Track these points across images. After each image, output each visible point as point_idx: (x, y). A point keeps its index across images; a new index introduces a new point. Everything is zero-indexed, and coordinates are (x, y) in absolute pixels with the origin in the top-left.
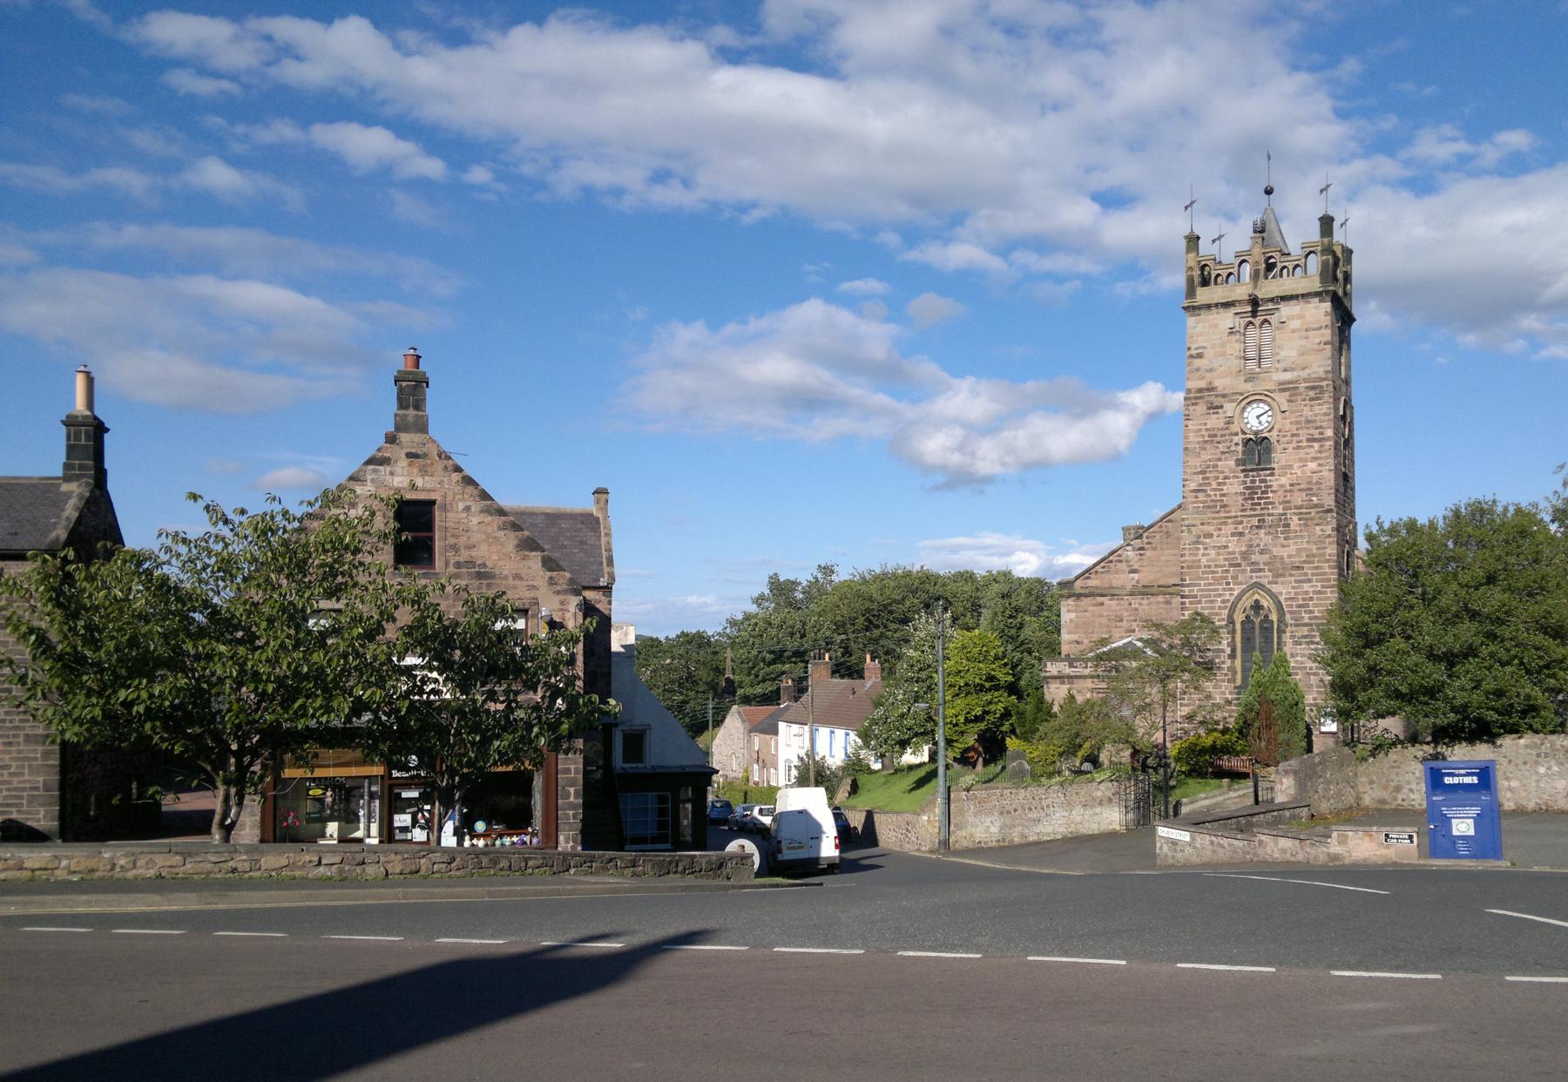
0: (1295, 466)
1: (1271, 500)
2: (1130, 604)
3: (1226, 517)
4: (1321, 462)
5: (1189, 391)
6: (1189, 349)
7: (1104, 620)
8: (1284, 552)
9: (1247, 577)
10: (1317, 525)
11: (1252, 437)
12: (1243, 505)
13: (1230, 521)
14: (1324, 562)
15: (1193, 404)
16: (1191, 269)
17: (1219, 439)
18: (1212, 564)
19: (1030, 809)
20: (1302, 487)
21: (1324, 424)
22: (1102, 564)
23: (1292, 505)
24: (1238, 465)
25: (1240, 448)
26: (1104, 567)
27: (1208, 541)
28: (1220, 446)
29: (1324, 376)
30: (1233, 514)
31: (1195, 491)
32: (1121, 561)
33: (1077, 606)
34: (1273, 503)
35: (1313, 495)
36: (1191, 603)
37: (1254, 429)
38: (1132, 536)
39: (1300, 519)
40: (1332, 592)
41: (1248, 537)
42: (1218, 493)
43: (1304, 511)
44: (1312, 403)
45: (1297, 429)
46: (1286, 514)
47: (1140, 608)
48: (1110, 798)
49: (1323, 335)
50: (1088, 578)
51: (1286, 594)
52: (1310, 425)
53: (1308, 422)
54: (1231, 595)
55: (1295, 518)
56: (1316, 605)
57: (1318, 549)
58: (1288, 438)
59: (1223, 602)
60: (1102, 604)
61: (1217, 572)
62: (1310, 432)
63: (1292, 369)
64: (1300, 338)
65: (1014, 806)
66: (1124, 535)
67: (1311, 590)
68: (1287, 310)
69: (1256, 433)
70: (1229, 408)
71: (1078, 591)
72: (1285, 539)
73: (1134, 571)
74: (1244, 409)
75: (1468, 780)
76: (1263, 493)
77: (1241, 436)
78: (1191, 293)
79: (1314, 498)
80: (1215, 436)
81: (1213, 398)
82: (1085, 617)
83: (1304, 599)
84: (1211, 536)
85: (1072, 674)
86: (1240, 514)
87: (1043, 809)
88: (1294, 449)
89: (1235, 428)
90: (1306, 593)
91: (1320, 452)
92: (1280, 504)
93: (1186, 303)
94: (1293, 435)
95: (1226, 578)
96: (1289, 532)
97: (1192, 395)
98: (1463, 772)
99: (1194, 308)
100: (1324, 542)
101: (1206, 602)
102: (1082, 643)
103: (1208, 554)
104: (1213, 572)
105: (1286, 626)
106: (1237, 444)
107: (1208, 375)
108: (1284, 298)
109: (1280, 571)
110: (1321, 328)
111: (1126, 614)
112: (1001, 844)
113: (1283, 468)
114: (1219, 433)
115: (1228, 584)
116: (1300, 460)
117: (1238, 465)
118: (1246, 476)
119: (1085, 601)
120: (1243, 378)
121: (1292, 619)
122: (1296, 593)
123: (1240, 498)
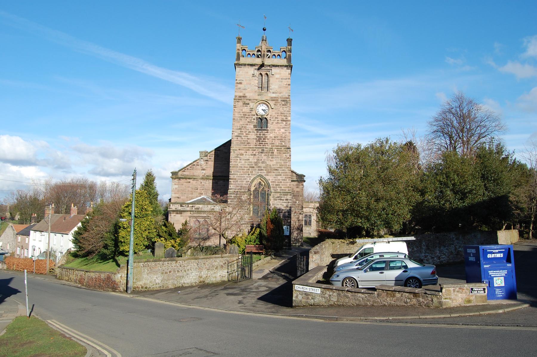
0: (276, 130)
1: (267, 142)
2: (201, 183)
4: (286, 129)
5: (236, 96)
6: (236, 80)
7: (190, 189)
8: (271, 163)
9: (256, 172)
10: (284, 153)
11: (260, 117)
12: (256, 144)
13: (250, 149)
15: (237, 102)
16: (239, 50)
17: (247, 116)
19: (178, 271)
20: (278, 138)
21: (287, 115)
22: (190, 166)
23: (275, 145)
24: (254, 128)
25: (255, 121)
26: (191, 167)
27: (241, 156)
28: (247, 119)
29: (288, 97)
30: (252, 147)
31: (236, 136)
32: (198, 165)
33: (179, 182)
34: (268, 144)
36: (233, 182)
37: (261, 114)
38: (203, 155)
39: (277, 151)
40: (289, 180)
41: (257, 156)
42: (246, 138)
43: (279, 147)
44: (283, 106)
45: (277, 116)
46: (272, 148)
48: (222, 266)
49: (288, 82)
50: (184, 171)
51: (272, 180)
52: (282, 115)
53: (282, 113)
54: (250, 179)
55: (276, 150)
56: (283, 185)
57: (284, 163)
59: (247, 182)
60: (190, 182)
61: (245, 170)
63: (276, 93)
65: (170, 270)
66: (200, 155)
67: (281, 179)
68: (274, 70)
69: (262, 116)
70: (252, 105)
71: (180, 176)
72: (272, 158)
73: (203, 170)
74: (257, 106)
75: (498, 255)
76: (263, 139)
78: (238, 58)
79: (283, 143)
80: (246, 115)
81: (245, 100)
82: (182, 187)
83: (278, 182)
84: (243, 155)
85: (181, 210)
86: (254, 147)
87: (185, 271)
88: (276, 123)
89: (254, 113)
90: (279, 180)
91: (286, 125)
92: (270, 144)
94: (276, 118)
96: (273, 155)
97: (237, 98)
98: (497, 251)
99: (239, 65)
100: (286, 160)
101: (240, 182)
102: (180, 198)
103: (241, 162)
104: (243, 169)
105: (271, 192)
106: (254, 119)
107: (244, 91)
108: (274, 66)
109: (270, 171)
110: (287, 79)
111: (199, 187)
113: (272, 130)
114: (247, 114)
115: (249, 174)
116: (278, 128)
118: (257, 132)
119: (182, 181)
123: (255, 141)
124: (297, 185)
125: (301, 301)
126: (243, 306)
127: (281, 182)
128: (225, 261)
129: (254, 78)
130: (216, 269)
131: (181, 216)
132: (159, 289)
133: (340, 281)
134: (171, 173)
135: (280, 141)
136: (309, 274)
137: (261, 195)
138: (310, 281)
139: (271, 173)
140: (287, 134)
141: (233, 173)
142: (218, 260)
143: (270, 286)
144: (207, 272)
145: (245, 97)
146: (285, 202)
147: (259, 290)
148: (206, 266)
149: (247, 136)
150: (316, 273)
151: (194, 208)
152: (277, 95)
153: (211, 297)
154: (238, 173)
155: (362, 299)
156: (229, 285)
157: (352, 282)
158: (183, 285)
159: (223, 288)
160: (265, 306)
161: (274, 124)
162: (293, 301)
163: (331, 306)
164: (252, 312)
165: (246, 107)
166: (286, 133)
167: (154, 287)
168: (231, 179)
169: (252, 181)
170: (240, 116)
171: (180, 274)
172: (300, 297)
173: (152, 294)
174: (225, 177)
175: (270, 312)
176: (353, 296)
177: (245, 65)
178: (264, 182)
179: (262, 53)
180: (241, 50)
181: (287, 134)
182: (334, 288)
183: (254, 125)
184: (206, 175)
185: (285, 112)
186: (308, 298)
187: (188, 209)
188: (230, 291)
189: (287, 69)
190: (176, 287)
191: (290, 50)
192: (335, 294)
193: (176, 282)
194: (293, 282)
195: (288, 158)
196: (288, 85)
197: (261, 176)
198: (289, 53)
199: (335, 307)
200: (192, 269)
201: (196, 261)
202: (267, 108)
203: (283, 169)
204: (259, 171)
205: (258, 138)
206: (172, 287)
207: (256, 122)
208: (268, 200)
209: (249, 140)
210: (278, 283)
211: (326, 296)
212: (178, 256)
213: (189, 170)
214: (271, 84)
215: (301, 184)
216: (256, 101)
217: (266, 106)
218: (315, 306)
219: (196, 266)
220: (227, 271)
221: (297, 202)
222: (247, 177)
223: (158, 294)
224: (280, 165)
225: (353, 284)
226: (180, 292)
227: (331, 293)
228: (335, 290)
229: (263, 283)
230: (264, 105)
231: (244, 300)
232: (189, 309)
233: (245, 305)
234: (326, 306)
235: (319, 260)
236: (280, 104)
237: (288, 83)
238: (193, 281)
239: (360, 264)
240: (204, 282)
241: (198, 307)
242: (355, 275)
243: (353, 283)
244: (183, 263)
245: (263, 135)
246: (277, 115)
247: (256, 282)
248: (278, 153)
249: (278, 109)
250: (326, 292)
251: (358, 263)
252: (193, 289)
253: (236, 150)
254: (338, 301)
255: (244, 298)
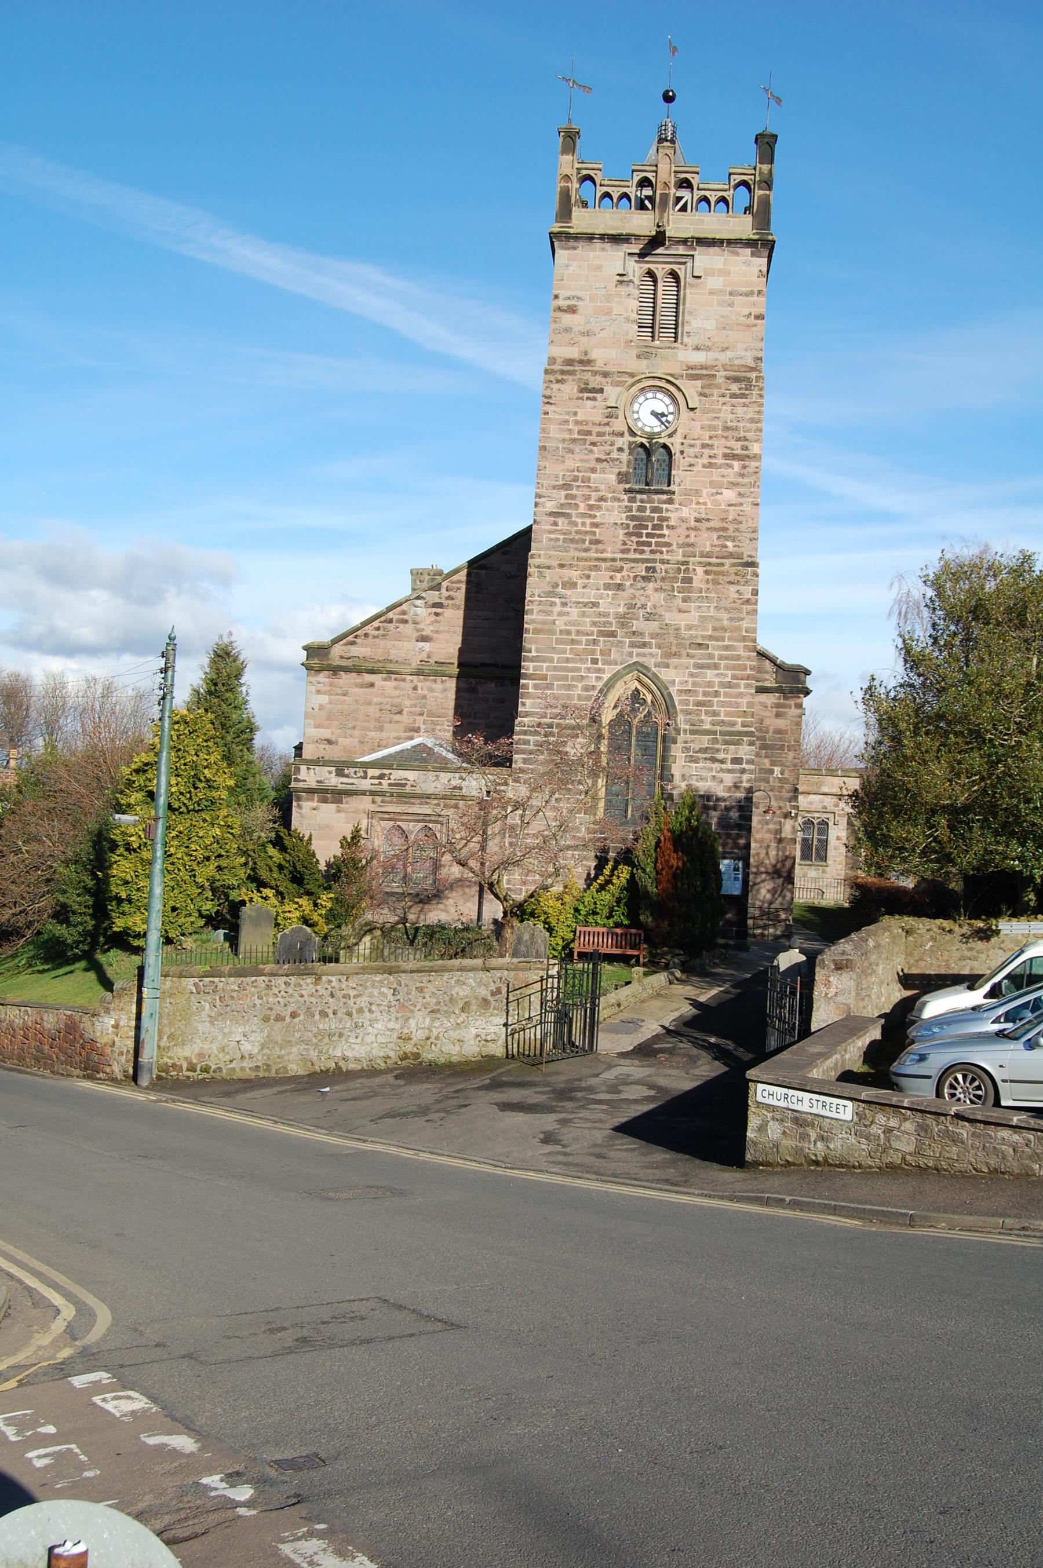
0: (705, 492)
1: (666, 540)
2: (415, 688)
3: (598, 559)
4: (742, 490)
5: (552, 360)
6: (556, 297)
7: (372, 710)
8: (682, 621)
9: (623, 653)
10: (731, 583)
11: (645, 441)
12: (625, 544)
13: (603, 565)
14: (739, 641)
15: (558, 381)
16: (567, 178)
17: (594, 438)
18: (573, 629)
20: (712, 524)
21: (749, 435)
22: (376, 624)
24: (620, 482)
25: (624, 457)
26: (378, 629)
27: (569, 592)
28: (595, 449)
29: (753, 365)
30: (609, 555)
31: (552, 514)
32: (406, 622)
35: (727, 538)
36: (536, 687)
37: (647, 429)
38: (425, 585)
39: (707, 573)
40: (747, 686)
42: (588, 521)
43: (714, 560)
45: (711, 438)
46: (687, 563)
47: (429, 695)
48: (485, 1001)
50: (353, 643)
52: (730, 434)
53: (727, 428)
54: (598, 678)
55: (700, 570)
56: (722, 704)
57: (731, 619)
58: (697, 450)
59: (586, 689)
60: (372, 685)
61: (579, 642)
62: (728, 444)
63: (708, 349)
64: (720, 304)
66: (414, 582)
67: (717, 680)
68: (704, 259)
69: (651, 437)
70: (612, 394)
71: (337, 662)
72: (685, 600)
73: (424, 639)
74: (636, 397)
76: (654, 527)
77: (628, 438)
78: (565, 213)
79: (730, 544)
80: (589, 433)
81: (588, 376)
83: (705, 694)
84: (574, 585)
85: (340, 787)
86: (619, 556)
87: (349, 1014)
88: (704, 466)
89: (619, 425)
90: (710, 684)
91: (742, 475)
92: (679, 546)
93: (556, 228)
94: (704, 446)
95: (593, 652)
97: (556, 367)
100: (740, 611)
101: (560, 687)
104: (573, 642)
106: (620, 450)
107: (584, 340)
108: (703, 242)
109: (674, 649)
110: (752, 293)
111: (408, 703)
112: (261, 1075)
113: (687, 493)
115: (595, 661)
116: (712, 484)
117: (620, 482)
118: (632, 500)
119: (346, 679)
120: (634, 352)
121: (686, 722)
122: (694, 684)
123: (622, 532)
124: (777, 706)
125: (777, 1146)
126: (558, 1153)
127: (716, 694)
128: (498, 984)
129: (624, 290)
130: (463, 1010)
131: (339, 811)
132: (253, 1075)
133: (929, 1077)
134: (306, 648)
135: (719, 537)
136: (811, 1047)
137: (637, 741)
138: (815, 1074)
139: (680, 656)
140: (747, 508)
141: (534, 654)
142: (471, 979)
143: (663, 1082)
144: (428, 1020)
145: (589, 362)
146: (729, 771)
147: (622, 1096)
148: (428, 999)
149: (590, 516)
150: (839, 1043)
151: (385, 782)
152: (712, 355)
153: (442, 1115)
154: (556, 656)
155: (1011, 1150)
156: (508, 1072)
157: (976, 1083)
158: (342, 1064)
159: (488, 1081)
160: (643, 1159)
161: (699, 468)
162: (749, 1145)
163: (892, 1170)
164: (593, 1177)
165: (589, 402)
166: (741, 504)
167: (234, 1069)
168: (528, 677)
169: (605, 685)
170: (567, 436)
171: (331, 1024)
172: (774, 1131)
173: (227, 1094)
174: (504, 667)
175: (658, 1181)
176: (979, 1136)
177: (590, 237)
178: (651, 692)
179: (658, 192)
180: (574, 179)
181: (747, 508)
182: (905, 1105)
183: (619, 474)
184: (432, 661)
185: (741, 425)
186: (804, 1137)
187: (366, 784)
188: (514, 1095)
189: (753, 255)
190: (315, 1073)
191: (766, 178)
192: (908, 1126)
193: (313, 1054)
194: (751, 1074)
195: (748, 601)
196: (757, 317)
197: (640, 668)
198: (762, 192)
199: (908, 1173)
200: (374, 1008)
201: (391, 978)
202: (671, 409)
203: (726, 643)
204: (635, 650)
205: (632, 524)
206: (301, 1072)
207: (629, 462)
208: (664, 758)
209: (597, 530)
210: (691, 1071)
211: (875, 1130)
212: (325, 959)
213: (370, 640)
214: (690, 313)
215: (792, 702)
216: (631, 381)
217: (667, 400)
218: (830, 1165)
219: (391, 998)
220: (503, 1021)
221: (777, 770)
222: (589, 670)
223: (249, 1095)
224: (715, 629)
225: (979, 1092)
226: (327, 1089)
227: (893, 1123)
228: (909, 1112)
229: (637, 1070)
230: (660, 395)
231: (565, 1130)
232: (359, 1154)
233: (568, 1150)
234: (870, 1167)
235: (853, 993)
236: (723, 391)
237: (755, 311)
238: (378, 1052)
239: (1009, 1017)
240: (417, 1056)
241: (392, 1150)
242: (988, 1058)
243: (979, 1088)
244: (343, 986)
245: (654, 510)
246: (708, 434)
247: (610, 1067)
248: (707, 581)
249: (713, 411)
250: (874, 1117)
251: (1002, 1011)
252: (377, 1080)
253: (549, 567)
254: (917, 1153)
255: (563, 1122)
